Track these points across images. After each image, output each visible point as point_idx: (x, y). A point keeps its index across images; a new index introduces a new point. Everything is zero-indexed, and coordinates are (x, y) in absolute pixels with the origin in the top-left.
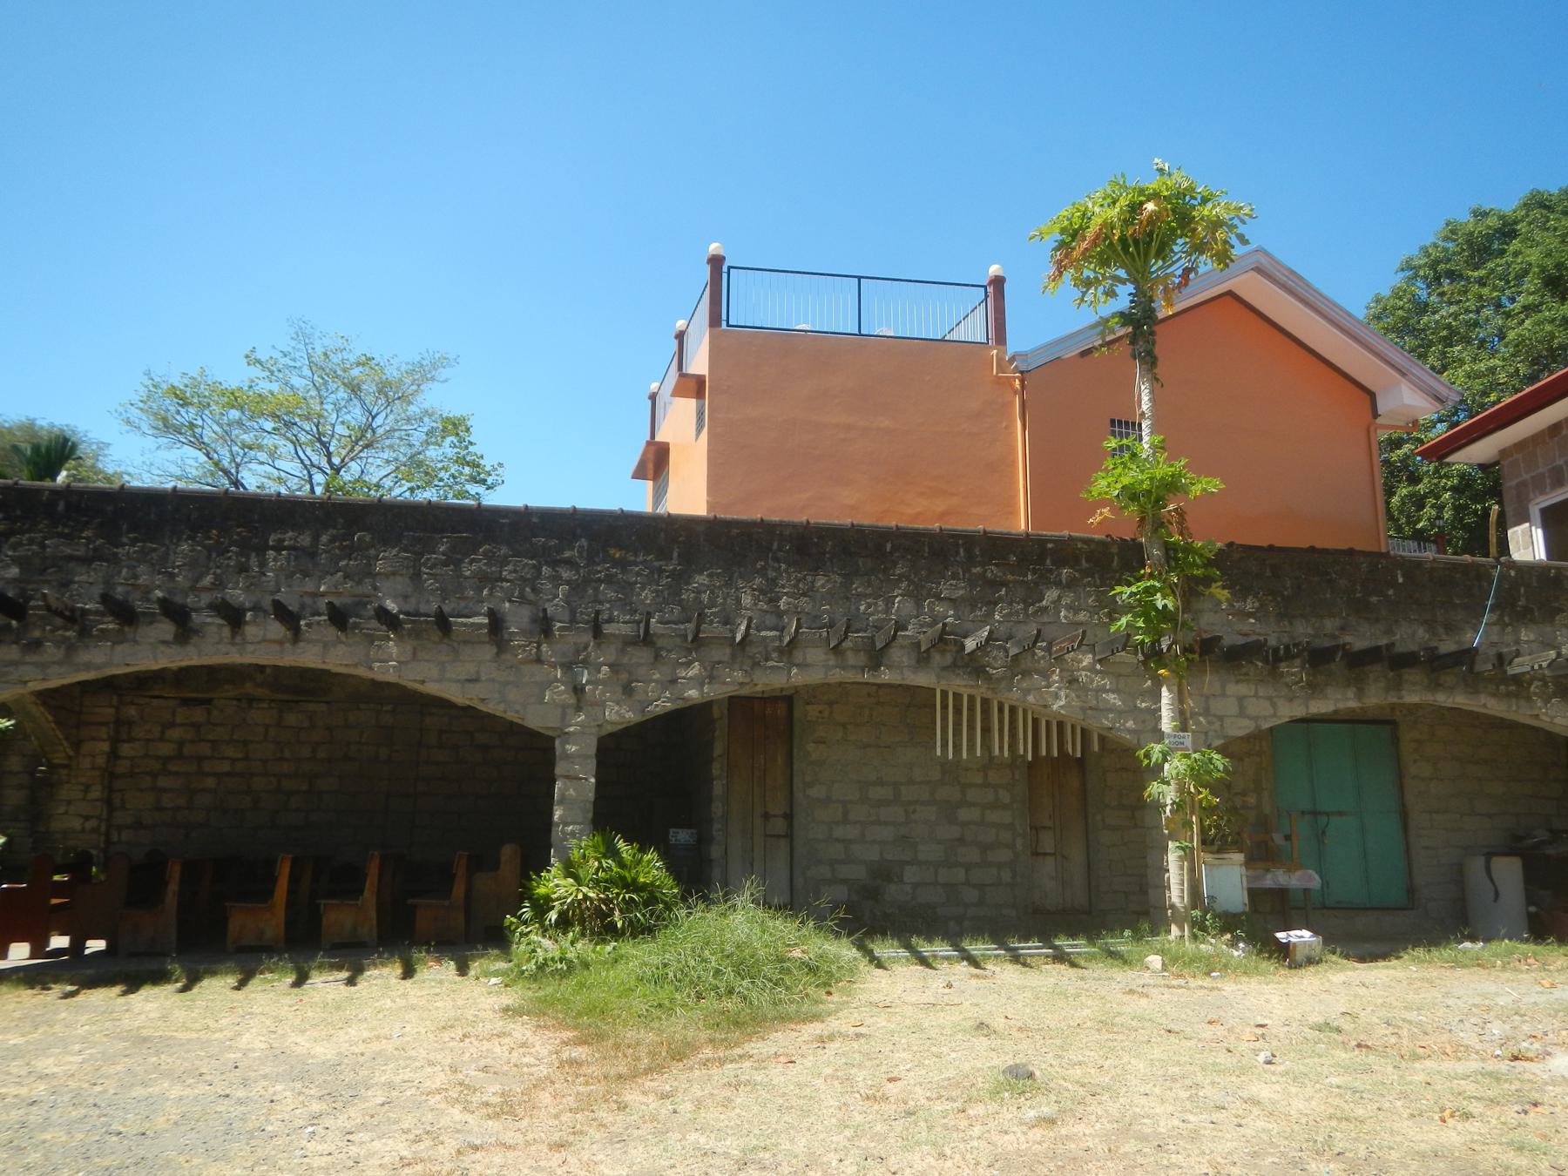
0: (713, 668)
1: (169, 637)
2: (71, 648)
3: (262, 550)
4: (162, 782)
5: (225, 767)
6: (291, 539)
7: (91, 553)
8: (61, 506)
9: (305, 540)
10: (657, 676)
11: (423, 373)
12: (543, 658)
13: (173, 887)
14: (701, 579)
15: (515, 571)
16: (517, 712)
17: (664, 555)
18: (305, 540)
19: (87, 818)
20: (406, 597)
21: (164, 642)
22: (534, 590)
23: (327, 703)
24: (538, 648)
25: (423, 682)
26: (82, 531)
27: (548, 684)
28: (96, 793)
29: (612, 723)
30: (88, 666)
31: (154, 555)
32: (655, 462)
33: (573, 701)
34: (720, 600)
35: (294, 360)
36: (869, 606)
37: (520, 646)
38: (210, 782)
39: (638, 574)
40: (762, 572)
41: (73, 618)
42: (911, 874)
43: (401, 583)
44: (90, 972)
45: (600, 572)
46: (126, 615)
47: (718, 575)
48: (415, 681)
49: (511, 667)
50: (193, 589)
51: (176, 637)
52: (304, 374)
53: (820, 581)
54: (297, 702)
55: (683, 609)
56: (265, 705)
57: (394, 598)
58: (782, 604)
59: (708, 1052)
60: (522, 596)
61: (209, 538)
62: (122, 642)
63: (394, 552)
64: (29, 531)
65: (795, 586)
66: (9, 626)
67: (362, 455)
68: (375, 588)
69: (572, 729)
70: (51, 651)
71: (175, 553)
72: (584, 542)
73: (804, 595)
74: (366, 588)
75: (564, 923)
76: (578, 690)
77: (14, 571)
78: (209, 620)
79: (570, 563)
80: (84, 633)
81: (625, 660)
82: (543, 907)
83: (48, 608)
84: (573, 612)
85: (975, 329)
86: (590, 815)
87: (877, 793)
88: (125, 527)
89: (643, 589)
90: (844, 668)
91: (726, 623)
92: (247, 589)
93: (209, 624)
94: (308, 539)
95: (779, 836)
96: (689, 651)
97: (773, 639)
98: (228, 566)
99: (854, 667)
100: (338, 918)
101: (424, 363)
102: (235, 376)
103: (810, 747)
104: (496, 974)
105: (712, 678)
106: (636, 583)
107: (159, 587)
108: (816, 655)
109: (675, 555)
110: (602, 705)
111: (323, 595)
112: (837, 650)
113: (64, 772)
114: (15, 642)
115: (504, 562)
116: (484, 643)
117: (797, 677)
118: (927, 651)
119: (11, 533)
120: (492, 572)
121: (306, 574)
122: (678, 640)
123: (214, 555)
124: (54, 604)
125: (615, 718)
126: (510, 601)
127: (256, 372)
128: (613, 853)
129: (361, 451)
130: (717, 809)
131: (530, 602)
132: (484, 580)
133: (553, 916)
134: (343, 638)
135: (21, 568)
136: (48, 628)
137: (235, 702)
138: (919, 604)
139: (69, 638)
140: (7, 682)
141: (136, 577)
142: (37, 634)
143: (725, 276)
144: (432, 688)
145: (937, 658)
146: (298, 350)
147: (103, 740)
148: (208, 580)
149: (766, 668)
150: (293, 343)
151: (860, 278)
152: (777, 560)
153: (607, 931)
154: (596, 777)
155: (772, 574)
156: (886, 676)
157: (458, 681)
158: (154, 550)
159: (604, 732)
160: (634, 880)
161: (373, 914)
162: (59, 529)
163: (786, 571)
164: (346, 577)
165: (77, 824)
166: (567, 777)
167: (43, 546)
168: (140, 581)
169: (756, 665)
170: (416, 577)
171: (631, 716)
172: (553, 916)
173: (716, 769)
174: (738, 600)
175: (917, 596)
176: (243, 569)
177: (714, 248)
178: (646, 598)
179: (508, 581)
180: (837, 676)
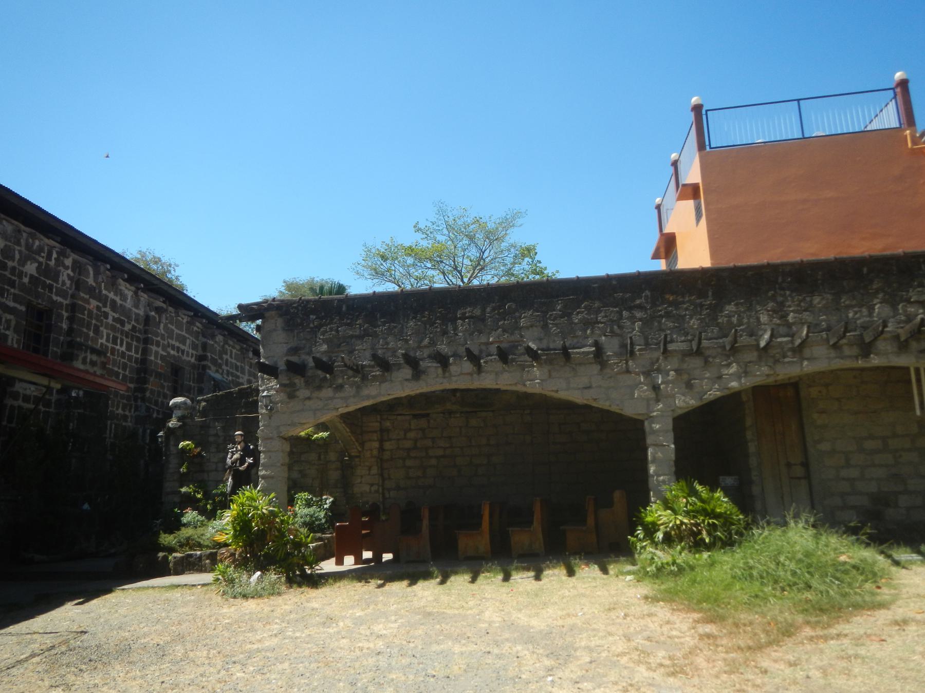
0: (746, 366)
1: (409, 376)
2: (359, 388)
3: (454, 320)
4: (409, 463)
5: (440, 452)
6: (469, 312)
7: (362, 333)
8: (344, 308)
9: (478, 312)
10: (708, 375)
11: (508, 223)
12: (630, 369)
13: (425, 523)
14: (730, 308)
15: (606, 316)
16: (618, 405)
17: (702, 294)
18: (478, 312)
19: (372, 485)
20: (540, 340)
21: (406, 380)
22: (620, 327)
23: (493, 411)
24: (627, 363)
25: (557, 391)
26: (356, 321)
27: (637, 385)
28: (375, 470)
29: (680, 408)
30: (368, 397)
31: (396, 330)
32: (668, 246)
33: (653, 395)
34: (745, 321)
35: (438, 226)
36: (856, 313)
37: (615, 363)
38: (433, 462)
39: (686, 309)
40: (773, 299)
41: (358, 370)
42: (904, 501)
43: (536, 332)
44: (389, 572)
45: (661, 311)
46: (385, 366)
47: (742, 304)
48: (553, 391)
49: (611, 377)
50: (419, 347)
51: (413, 375)
52: (444, 233)
53: (816, 300)
54: (476, 412)
55: (721, 329)
56: (458, 415)
57: (534, 341)
58: (791, 318)
59: (808, 631)
60: (612, 331)
61: (424, 317)
62: (385, 382)
63: (530, 313)
64: (329, 324)
65: (799, 305)
66: (326, 377)
67: (479, 275)
68: (522, 336)
69: (655, 414)
70: (349, 390)
71: (407, 328)
72: (648, 293)
73: (806, 310)
74: (517, 337)
75: (668, 540)
76: (656, 388)
77: (325, 347)
78: (430, 365)
79: (640, 307)
80: (364, 378)
81: (685, 366)
82: (651, 531)
83: (345, 365)
84: (646, 339)
85: (889, 118)
86: (673, 469)
87: (870, 445)
88: (378, 315)
89: (691, 318)
90: (842, 358)
91: (751, 335)
92: (448, 344)
93: (429, 367)
94: (479, 311)
95: (799, 478)
96: (728, 356)
97: (787, 343)
98: (436, 332)
99: (850, 357)
100: (520, 538)
101: (508, 217)
102: (409, 238)
103: (815, 416)
104: (629, 573)
105: (746, 373)
106: (685, 315)
107: (400, 348)
108: (820, 351)
109: (710, 293)
110: (673, 397)
111: (492, 343)
112: (835, 346)
113: (357, 460)
114: (329, 387)
115: (598, 311)
116: (591, 363)
117: (807, 367)
118: (906, 341)
119: (320, 326)
120: (592, 319)
121: (480, 332)
122: (719, 350)
123: (428, 326)
124: (348, 363)
125: (682, 404)
126: (605, 336)
127: (420, 235)
128: (694, 493)
129: (478, 273)
130: (753, 461)
131: (617, 335)
132: (587, 324)
133: (660, 535)
134: (507, 368)
135: (328, 345)
136: (345, 377)
137: (442, 415)
138: (894, 306)
139: (357, 382)
140: (328, 409)
141: (387, 344)
142: (340, 381)
143: (704, 117)
144: (563, 395)
145: (914, 345)
146: (440, 220)
147: (376, 441)
148: (426, 341)
149: (784, 363)
150: (437, 216)
151: (798, 100)
152: (783, 289)
153: (698, 546)
154: (675, 443)
155: (780, 299)
156: (875, 361)
157: (579, 389)
158: (395, 327)
159: (676, 415)
160: (713, 510)
161: (540, 536)
162: (345, 321)
163: (790, 295)
164: (504, 331)
165: (366, 488)
166: (656, 445)
167: (337, 331)
168: (390, 346)
169: (777, 361)
170: (545, 327)
171: (693, 403)
172: (660, 535)
173: (749, 435)
174: (758, 319)
175: (892, 301)
176: (445, 333)
177: (695, 100)
178: (694, 324)
179: (602, 323)
180: (837, 364)
